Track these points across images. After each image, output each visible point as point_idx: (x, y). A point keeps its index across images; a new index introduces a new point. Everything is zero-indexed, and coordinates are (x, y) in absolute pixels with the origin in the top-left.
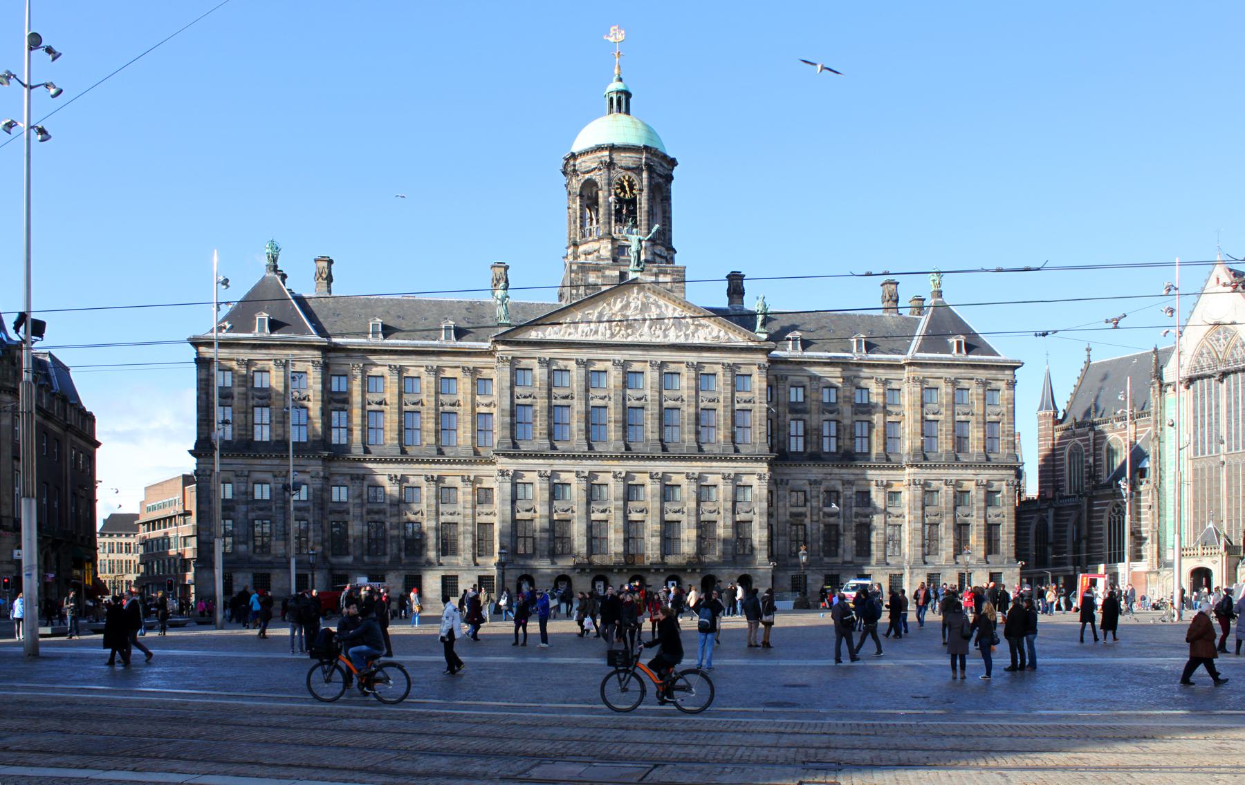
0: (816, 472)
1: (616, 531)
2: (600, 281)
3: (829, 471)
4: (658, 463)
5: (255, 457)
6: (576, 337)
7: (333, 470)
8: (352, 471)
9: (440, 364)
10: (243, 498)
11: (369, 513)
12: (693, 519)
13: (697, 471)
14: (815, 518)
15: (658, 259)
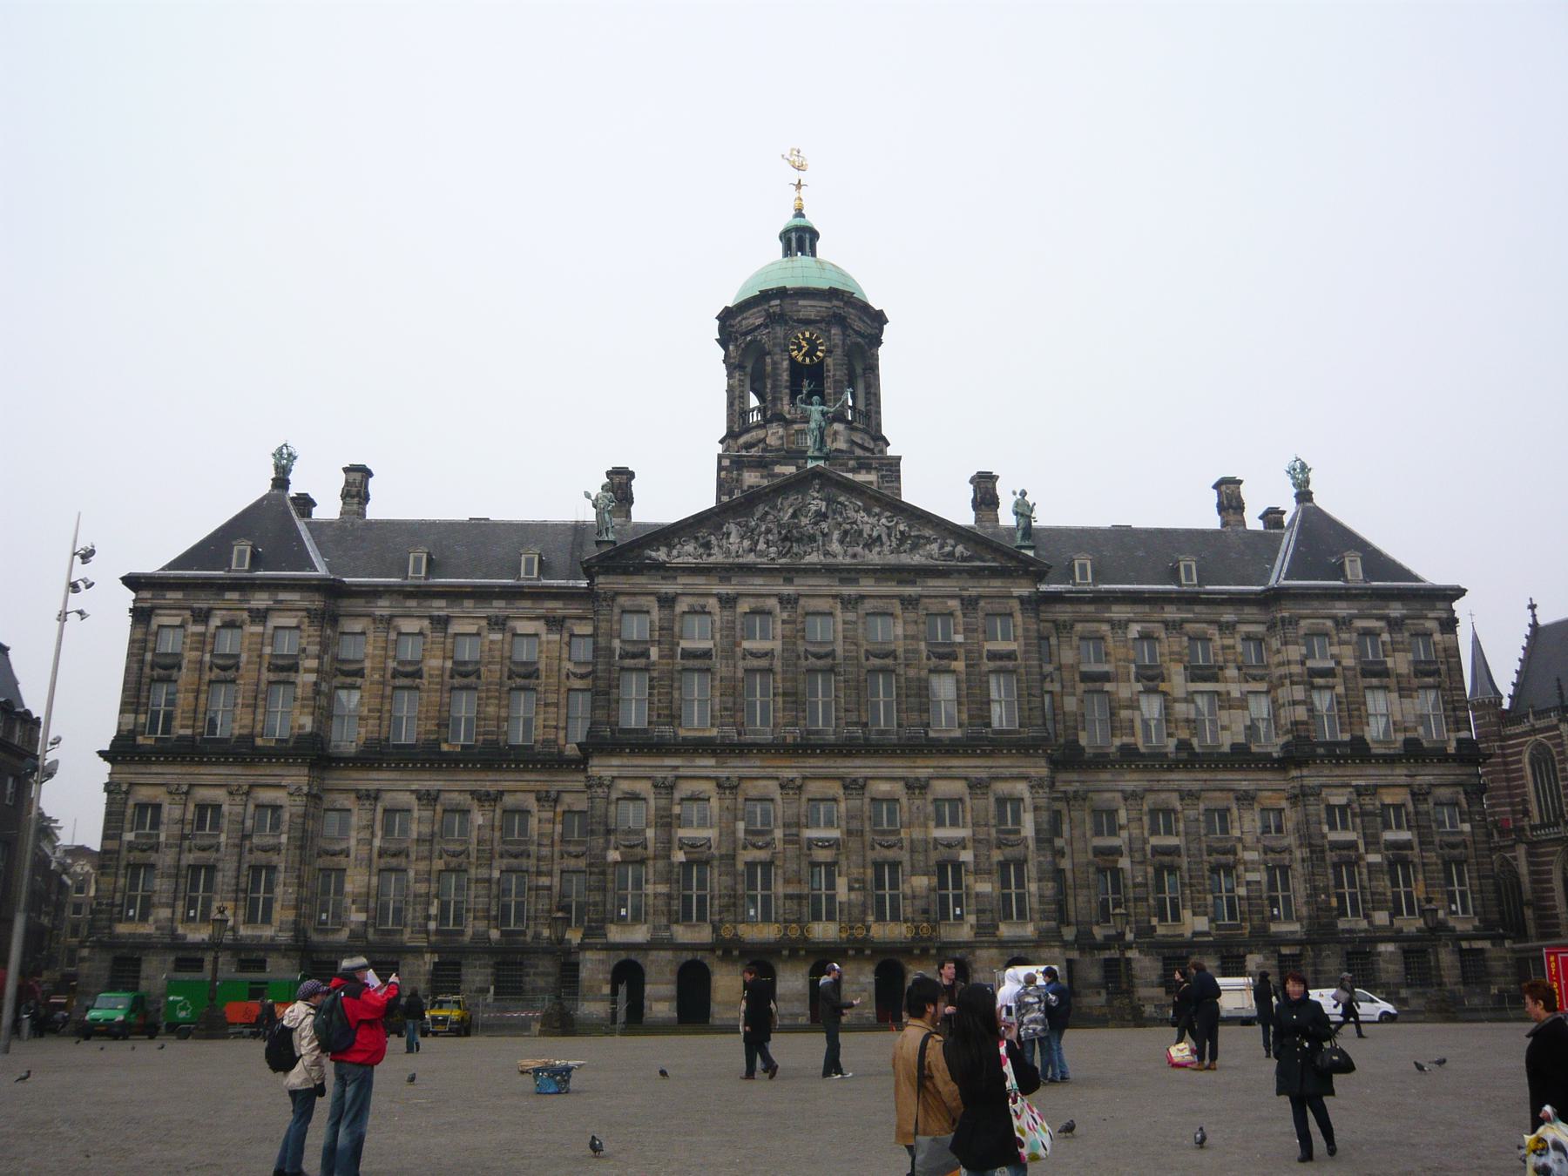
0: (1132, 781)
1: (787, 881)
2: (765, 482)
3: (1156, 776)
4: (858, 762)
5: (201, 763)
6: (717, 557)
7: (330, 783)
8: (363, 786)
9: (510, 612)
10: (176, 829)
11: (380, 855)
12: (921, 858)
13: (922, 773)
14: (1138, 857)
15: (859, 452)
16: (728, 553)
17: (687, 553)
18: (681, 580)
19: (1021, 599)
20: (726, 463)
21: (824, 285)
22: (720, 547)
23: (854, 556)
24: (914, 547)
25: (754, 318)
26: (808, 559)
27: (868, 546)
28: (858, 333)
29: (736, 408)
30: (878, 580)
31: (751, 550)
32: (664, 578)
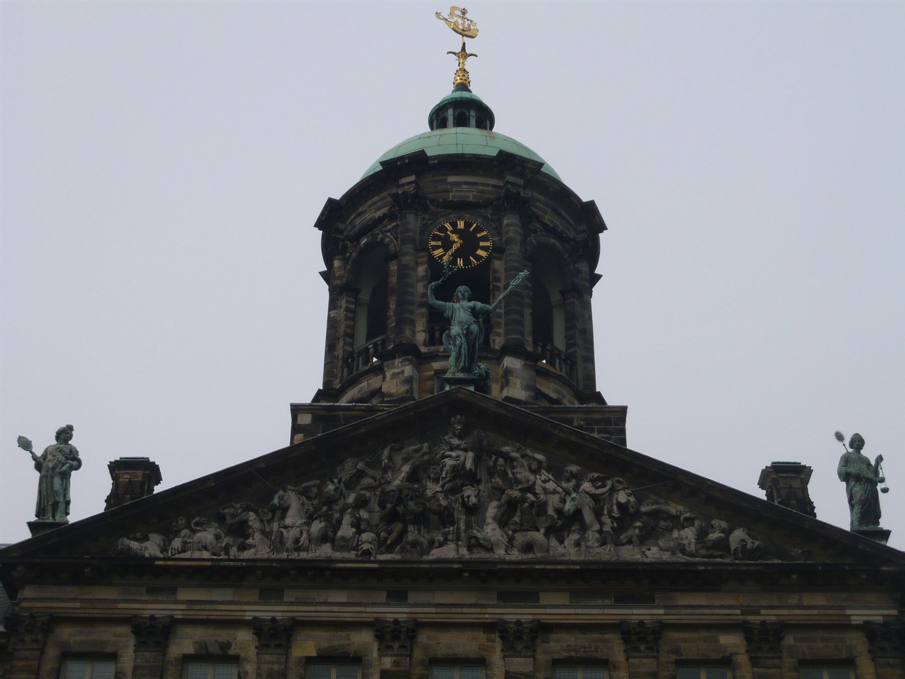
16: (279, 543)
17: (203, 542)
18: (184, 595)
19: (867, 628)
20: (305, 419)
21: (493, 153)
22: (264, 533)
23: (528, 547)
24: (648, 536)
25: (372, 211)
26: (436, 553)
27: (557, 531)
28: (551, 231)
29: (339, 353)
30: (577, 597)
31: (324, 538)
32: (151, 590)
